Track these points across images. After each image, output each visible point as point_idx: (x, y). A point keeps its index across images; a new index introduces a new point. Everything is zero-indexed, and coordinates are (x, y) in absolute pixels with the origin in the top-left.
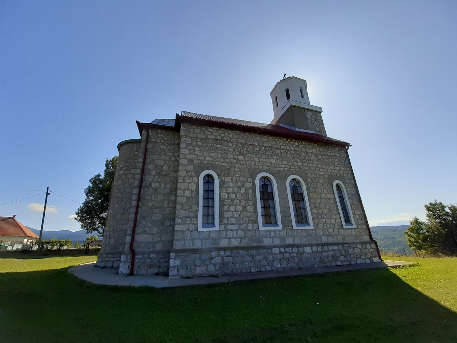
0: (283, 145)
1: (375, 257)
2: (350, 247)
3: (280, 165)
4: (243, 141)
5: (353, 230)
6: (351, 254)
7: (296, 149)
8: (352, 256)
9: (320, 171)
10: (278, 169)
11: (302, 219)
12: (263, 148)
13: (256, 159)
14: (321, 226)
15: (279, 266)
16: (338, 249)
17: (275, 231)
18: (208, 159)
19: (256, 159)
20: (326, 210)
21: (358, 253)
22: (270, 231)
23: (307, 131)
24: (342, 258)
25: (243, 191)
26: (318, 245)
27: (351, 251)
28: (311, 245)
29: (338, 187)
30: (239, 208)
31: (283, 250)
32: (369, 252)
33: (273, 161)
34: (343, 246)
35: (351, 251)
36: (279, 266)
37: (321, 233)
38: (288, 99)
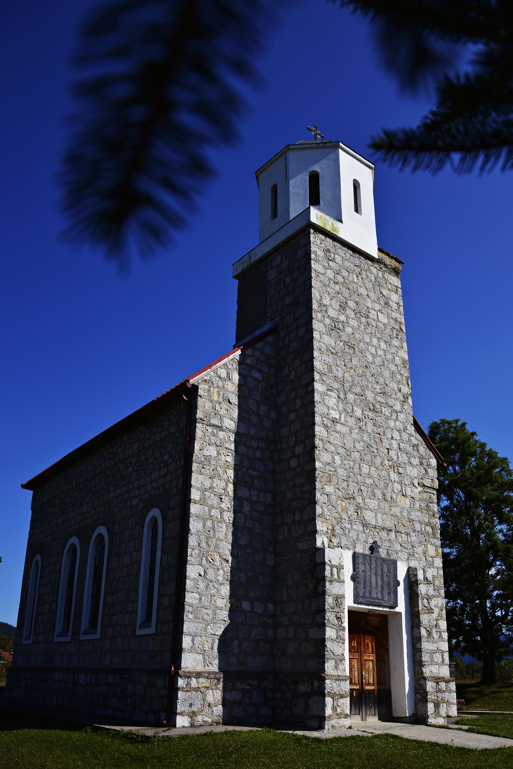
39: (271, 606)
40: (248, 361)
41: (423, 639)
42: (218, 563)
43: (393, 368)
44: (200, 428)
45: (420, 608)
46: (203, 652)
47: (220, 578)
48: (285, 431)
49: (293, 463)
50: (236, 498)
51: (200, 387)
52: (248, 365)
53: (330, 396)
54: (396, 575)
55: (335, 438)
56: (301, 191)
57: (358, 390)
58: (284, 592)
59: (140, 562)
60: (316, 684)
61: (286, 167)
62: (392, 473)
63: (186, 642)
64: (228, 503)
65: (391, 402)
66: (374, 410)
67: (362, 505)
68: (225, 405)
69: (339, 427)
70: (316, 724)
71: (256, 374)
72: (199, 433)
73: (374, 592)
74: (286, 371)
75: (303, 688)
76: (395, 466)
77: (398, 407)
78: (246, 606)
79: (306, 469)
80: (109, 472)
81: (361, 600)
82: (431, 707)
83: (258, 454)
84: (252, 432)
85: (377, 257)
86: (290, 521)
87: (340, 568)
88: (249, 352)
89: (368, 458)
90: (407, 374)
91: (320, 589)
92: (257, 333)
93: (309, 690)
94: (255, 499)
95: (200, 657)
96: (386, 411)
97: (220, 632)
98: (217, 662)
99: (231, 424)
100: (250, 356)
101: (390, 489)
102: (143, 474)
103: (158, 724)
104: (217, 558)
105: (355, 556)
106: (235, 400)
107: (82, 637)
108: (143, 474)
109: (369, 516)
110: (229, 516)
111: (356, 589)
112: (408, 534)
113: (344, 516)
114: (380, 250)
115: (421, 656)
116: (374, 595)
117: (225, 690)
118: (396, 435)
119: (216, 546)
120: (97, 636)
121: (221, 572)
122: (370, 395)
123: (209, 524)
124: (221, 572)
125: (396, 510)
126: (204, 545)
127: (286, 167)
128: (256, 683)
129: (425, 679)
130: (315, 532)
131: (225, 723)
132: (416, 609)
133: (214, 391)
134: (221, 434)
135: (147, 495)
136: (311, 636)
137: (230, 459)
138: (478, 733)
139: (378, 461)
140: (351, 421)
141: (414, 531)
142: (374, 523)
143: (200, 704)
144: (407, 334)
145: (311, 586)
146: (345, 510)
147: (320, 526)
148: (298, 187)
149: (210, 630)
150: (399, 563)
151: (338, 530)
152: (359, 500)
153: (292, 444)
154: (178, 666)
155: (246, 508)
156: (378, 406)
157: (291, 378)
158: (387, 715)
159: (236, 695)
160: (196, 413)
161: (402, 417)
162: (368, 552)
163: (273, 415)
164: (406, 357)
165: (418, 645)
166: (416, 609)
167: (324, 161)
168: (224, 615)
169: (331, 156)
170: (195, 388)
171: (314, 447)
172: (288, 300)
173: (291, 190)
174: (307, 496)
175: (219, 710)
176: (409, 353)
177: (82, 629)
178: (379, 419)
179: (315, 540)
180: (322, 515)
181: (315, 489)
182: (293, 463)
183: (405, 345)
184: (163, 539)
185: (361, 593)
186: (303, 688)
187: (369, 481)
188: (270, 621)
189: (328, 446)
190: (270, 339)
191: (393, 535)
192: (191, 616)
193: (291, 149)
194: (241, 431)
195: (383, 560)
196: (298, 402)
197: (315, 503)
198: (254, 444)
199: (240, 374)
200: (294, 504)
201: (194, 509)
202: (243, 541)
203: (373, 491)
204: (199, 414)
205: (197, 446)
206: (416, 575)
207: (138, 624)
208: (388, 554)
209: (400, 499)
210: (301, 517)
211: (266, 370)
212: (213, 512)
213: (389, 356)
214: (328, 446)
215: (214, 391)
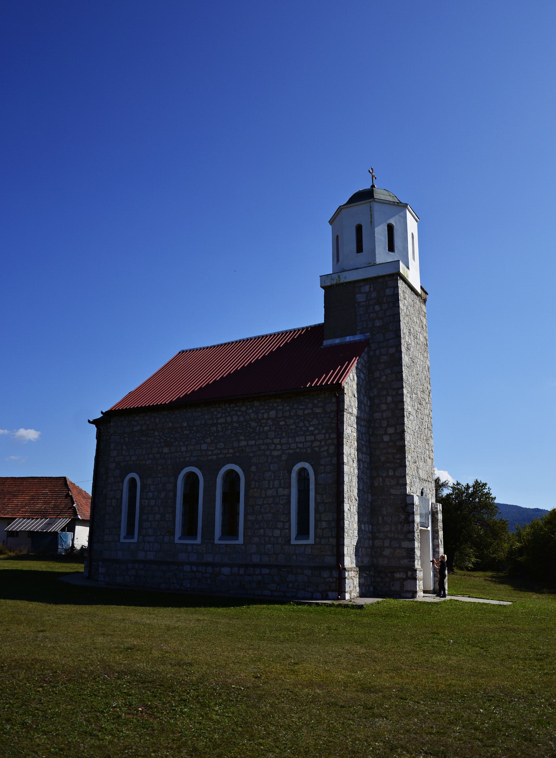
0: (221, 417)
3: (212, 451)
4: (170, 425)
7: (242, 419)
8: (291, 585)
9: (275, 449)
10: (210, 458)
11: (230, 529)
12: (195, 428)
13: (184, 449)
14: (256, 539)
15: (189, 586)
17: (192, 545)
18: (134, 458)
19: (184, 449)
22: (187, 545)
23: (348, 339)
25: (163, 495)
30: (158, 517)
31: (194, 568)
33: (204, 447)
36: (189, 586)
48: (377, 415)
50: (359, 461)
56: (383, 238)
58: (380, 518)
60: (410, 573)
61: (371, 215)
68: (353, 399)
70: (410, 595)
74: (377, 374)
75: (398, 575)
79: (398, 444)
80: (236, 425)
85: (420, 293)
86: (384, 475)
91: (410, 519)
93: (404, 577)
97: (355, 544)
102: (284, 435)
106: (356, 395)
108: (284, 435)
114: (421, 287)
124: (355, 507)
127: (371, 215)
132: (436, 528)
135: (291, 451)
138: (476, 598)
145: (403, 517)
148: (381, 234)
165: (437, 550)
166: (436, 528)
167: (397, 217)
169: (402, 214)
171: (403, 431)
172: (378, 323)
173: (376, 235)
174: (398, 461)
184: (316, 484)
186: (398, 575)
193: (376, 201)
196: (389, 399)
197: (405, 466)
200: (388, 465)
206: (437, 508)
210: (394, 474)
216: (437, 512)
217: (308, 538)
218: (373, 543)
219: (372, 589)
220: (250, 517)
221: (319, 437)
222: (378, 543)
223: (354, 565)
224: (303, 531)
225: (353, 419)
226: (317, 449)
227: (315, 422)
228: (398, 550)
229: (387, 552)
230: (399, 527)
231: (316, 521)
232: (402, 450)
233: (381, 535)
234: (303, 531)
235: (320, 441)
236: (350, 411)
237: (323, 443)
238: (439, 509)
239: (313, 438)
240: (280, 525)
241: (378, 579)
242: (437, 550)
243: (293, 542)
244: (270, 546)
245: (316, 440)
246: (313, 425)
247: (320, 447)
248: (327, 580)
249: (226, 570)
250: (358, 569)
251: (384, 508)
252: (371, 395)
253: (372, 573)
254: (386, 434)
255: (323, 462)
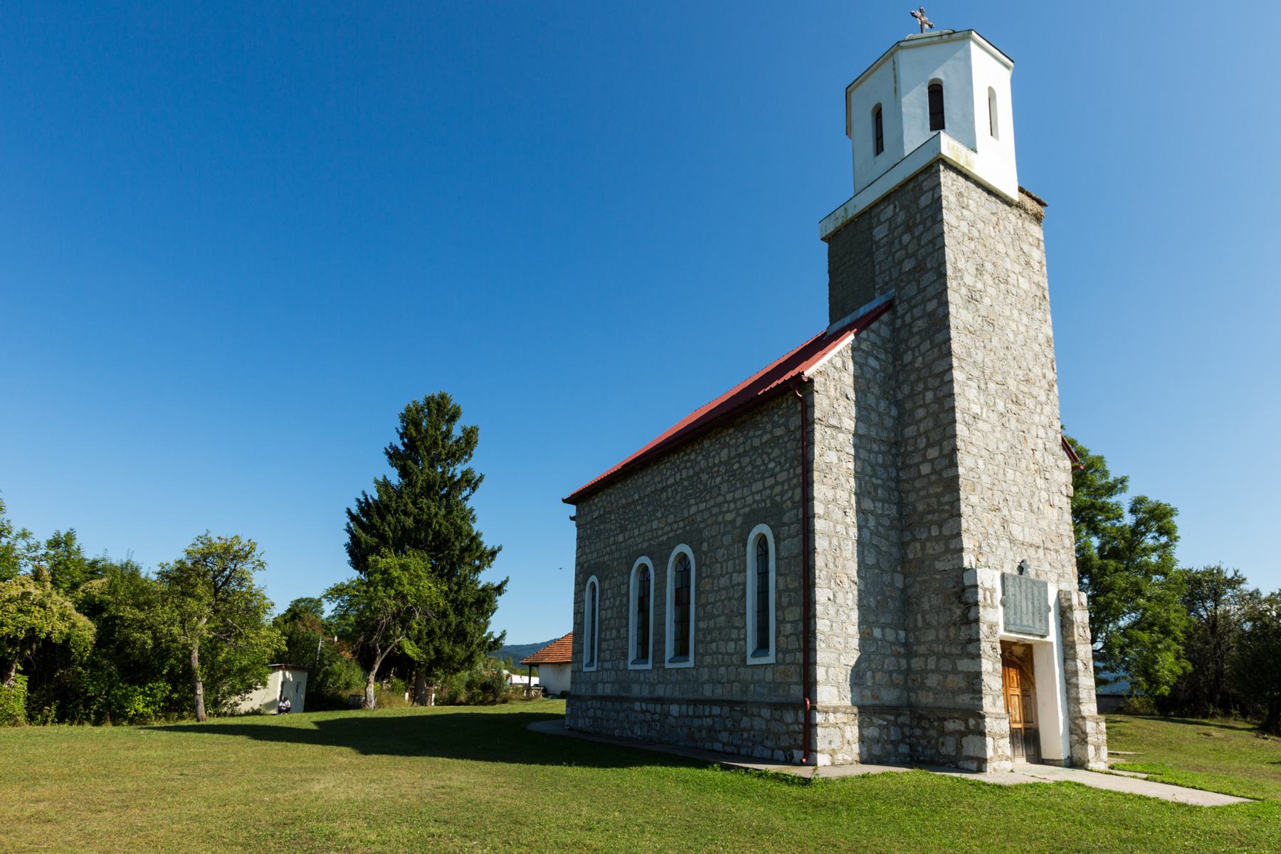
1: (799, 748)
2: (744, 713)
5: (770, 669)
6: (745, 730)
8: (745, 735)
16: (720, 716)
17: (644, 671)
20: (723, 618)
21: (760, 730)
24: (724, 736)
26: (689, 702)
27: (745, 722)
28: (679, 702)
29: (762, 541)
32: (788, 733)
34: (732, 709)
35: (745, 722)
37: (706, 677)
38: (932, 129)
39: (902, 634)
40: (864, 346)
41: (1080, 674)
42: (846, 586)
43: (1037, 348)
44: (819, 431)
45: (1076, 637)
46: (838, 685)
47: (850, 603)
48: (910, 431)
49: (925, 469)
50: (860, 511)
51: (816, 380)
52: (863, 351)
53: (970, 387)
54: (1046, 600)
55: (977, 438)
57: (999, 378)
58: (919, 617)
59: (745, 584)
62: (1038, 479)
63: (820, 673)
64: (852, 518)
65: (1035, 391)
66: (1017, 403)
67: (1008, 517)
68: (843, 402)
69: (980, 424)
71: (873, 362)
72: (818, 436)
73: (1025, 618)
74: (908, 357)
75: (951, 726)
76: (1042, 471)
77: (1043, 398)
78: (877, 633)
81: (1012, 628)
82: (1091, 749)
83: (880, 460)
84: (873, 434)
86: (923, 537)
87: (992, 591)
88: (864, 334)
89: (1012, 461)
90: (1052, 356)
92: (863, 310)
93: (963, 729)
94: (880, 512)
95: (835, 690)
96: (1030, 403)
97: (853, 663)
98: (849, 696)
99: (849, 424)
100: (865, 340)
101: (1036, 499)
103: (789, 761)
104: (845, 580)
105: (1003, 577)
106: (852, 395)
107: (668, 665)
109: (1016, 530)
110: (853, 532)
111: (1005, 614)
112: (1057, 551)
113: (991, 531)
115: (1078, 693)
116: (1025, 623)
117: (860, 727)
118: (1041, 432)
119: (844, 567)
120: (690, 663)
121: (850, 596)
122: (1011, 382)
123: (835, 541)
124: (850, 596)
125: (1043, 524)
126: (831, 565)
128: (892, 718)
129: (1084, 718)
130: (962, 549)
131: (863, 762)
133: (831, 385)
134: (841, 437)
136: (960, 668)
137: (851, 466)
139: (1023, 464)
140: (994, 417)
141: (1064, 548)
142: (1021, 538)
143: (838, 743)
144: (1051, 304)
145: (958, 612)
146: (991, 523)
147: (967, 542)
149: (843, 661)
150: (1049, 585)
151: (985, 548)
152: (1005, 512)
153: (922, 446)
154: (814, 701)
155: (872, 523)
156: (1021, 397)
157: (917, 365)
158: (1036, 757)
159: (872, 732)
160: (813, 413)
161: (1047, 409)
162: (1016, 573)
163: (894, 412)
164: (1051, 333)
165: (1073, 680)
168: (855, 642)
170: (811, 381)
171: (955, 450)
174: (947, 507)
175: (856, 748)
176: (1055, 327)
177: (667, 657)
178: (1022, 413)
179: (961, 559)
180: (968, 530)
181: (959, 500)
182: (925, 469)
183: (1049, 317)
184: (778, 559)
185: (1012, 621)
186: (951, 726)
187: (1015, 489)
188: (902, 650)
189: (970, 448)
190: (885, 317)
191: (1041, 551)
192: (823, 645)
194: (861, 432)
195: (1033, 582)
196: (929, 396)
197: (960, 516)
198: (875, 447)
199: (855, 363)
200: (930, 517)
201: (819, 525)
202: (871, 560)
203: (1019, 501)
204: (817, 414)
205: (817, 451)
206: (1070, 600)
207: (750, 651)
208: (1037, 575)
209: (1047, 509)
211: (882, 357)
212: (839, 528)
213: (1032, 333)
214: (970, 448)
215: (831, 385)
216: (1070, 607)
217: (767, 655)
218: (908, 664)
219: (904, 749)
220: (702, 625)
221: (781, 477)
222: (917, 663)
223: (848, 703)
224: (763, 645)
225: (846, 440)
226: (778, 498)
227: (777, 452)
228: (951, 677)
229: (932, 680)
230: (952, 631)
231: (779, 622)
232: (952, 485)
233: (922, 649)
234: (763, 645)
235: (782, 484)
236: (834, 422)
237: (786, 487)
238: (1075, 601)
239: (772, 481)
240: (734, 634)
241: (918, 732)
242: (1073, 680)
243: (750, 661)
244: (723, 669)
245: (777, 483)
246: (773, 460)
247: (782, 494)
248: (791, 728)
249: (674, 709)
250: (856, 710)
251: (925, 599)
252: (900, 396)
253: (901, 719)
254: (925, 460)
255: (786, 519)
